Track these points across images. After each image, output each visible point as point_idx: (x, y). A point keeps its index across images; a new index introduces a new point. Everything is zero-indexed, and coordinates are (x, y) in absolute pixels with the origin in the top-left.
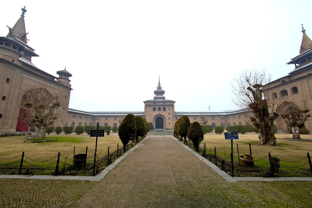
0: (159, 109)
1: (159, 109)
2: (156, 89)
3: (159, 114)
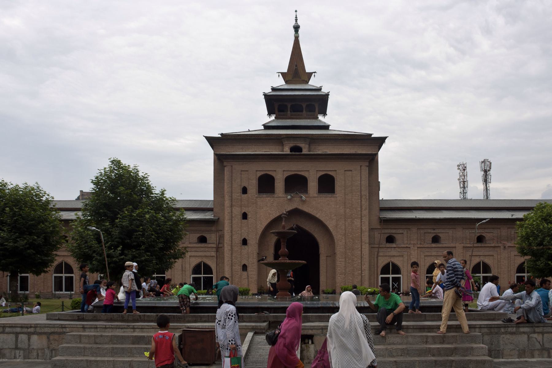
0: (296, 183)
1: (296, 183)
2: (280, 82)
3: (296, 213)
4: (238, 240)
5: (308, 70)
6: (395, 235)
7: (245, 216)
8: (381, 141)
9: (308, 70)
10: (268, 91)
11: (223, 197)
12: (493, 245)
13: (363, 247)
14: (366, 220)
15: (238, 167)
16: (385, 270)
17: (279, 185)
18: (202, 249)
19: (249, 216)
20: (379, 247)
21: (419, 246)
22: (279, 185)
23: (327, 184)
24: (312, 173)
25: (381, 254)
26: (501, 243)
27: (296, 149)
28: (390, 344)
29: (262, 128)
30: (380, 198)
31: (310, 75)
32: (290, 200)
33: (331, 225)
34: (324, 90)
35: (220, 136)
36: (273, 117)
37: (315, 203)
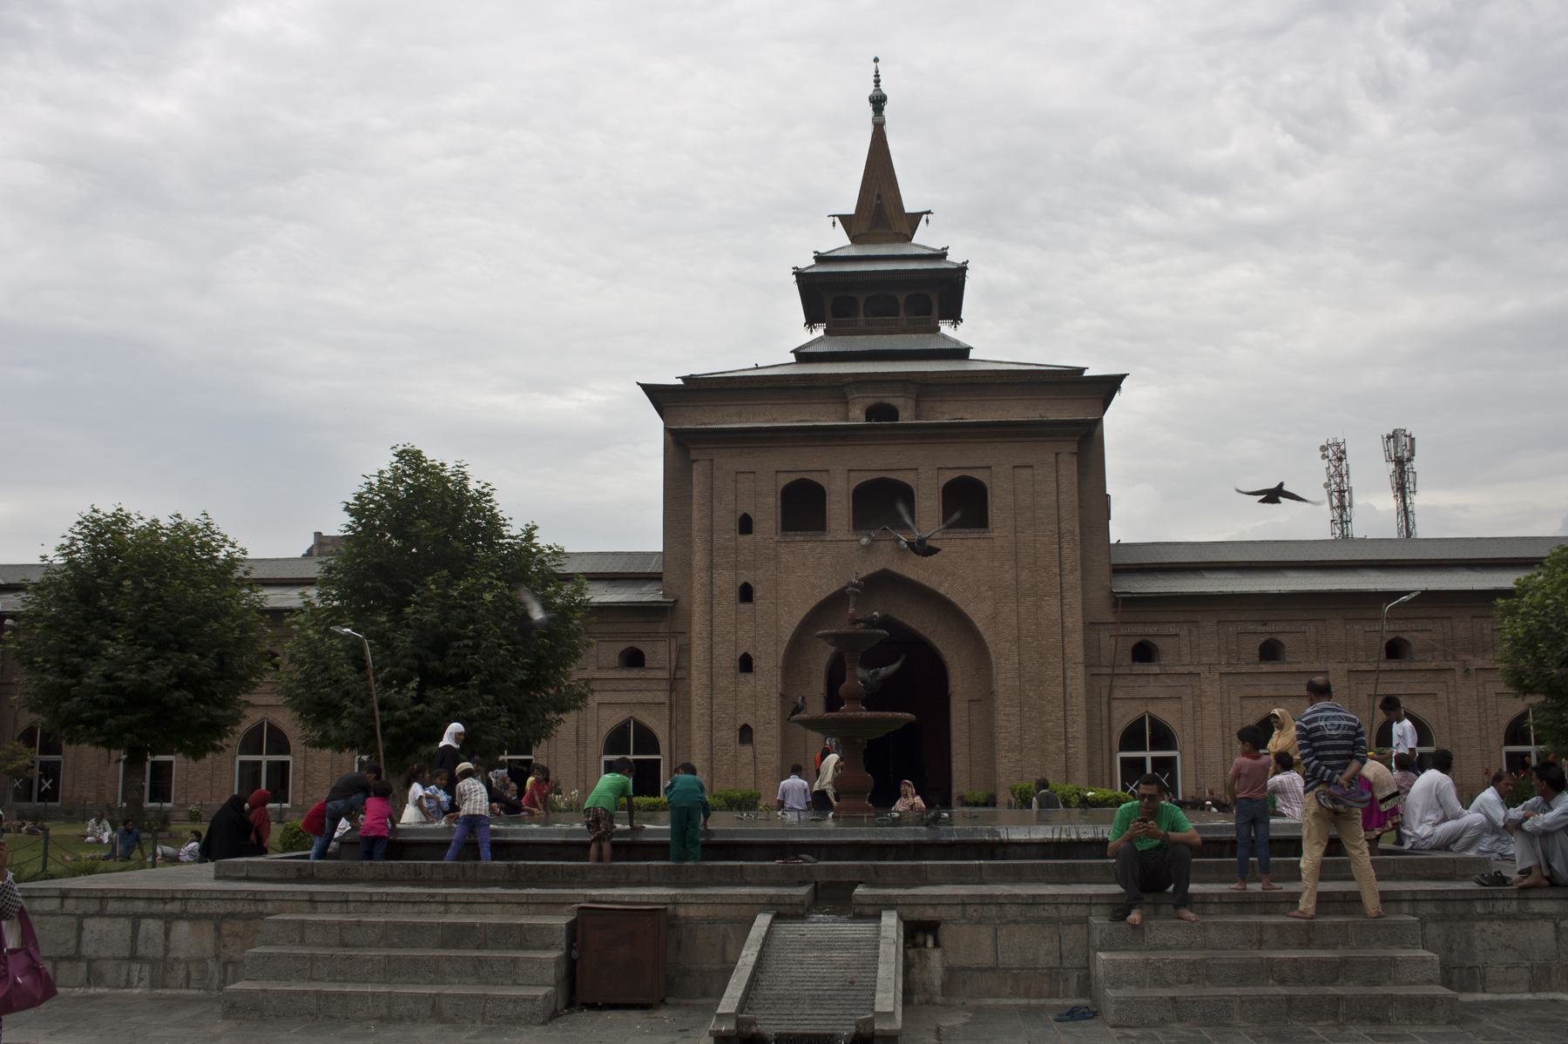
1: (880, 502)
2: (837, 240)
3: (884, 582)
4: (727, 658)
6: (1156, 641)
7: (746, 594)
8: (1110, 385)
10: (807, 262)
12: (1433, 665)
13: (1069, 673)
14: (1074, 600)
15: (729, 461)
16: (1132, 737)
17: (839, 508)
18: (632, 685)
19: (758, 593)
20: (1113, 675)
21: (1224, 669)
22: (839, 508)
23: (967, 503)
24: (927, 475)
25: (1118, 693)
26: (1454, 658)
28: (1154, 948)
29: (792, 359)
30: (1113, 540)
31: (915, 219)
32: (867, 547)
33: (978, 613)
34: (954, 258)
35: (680, 382)
36: (819, 332)
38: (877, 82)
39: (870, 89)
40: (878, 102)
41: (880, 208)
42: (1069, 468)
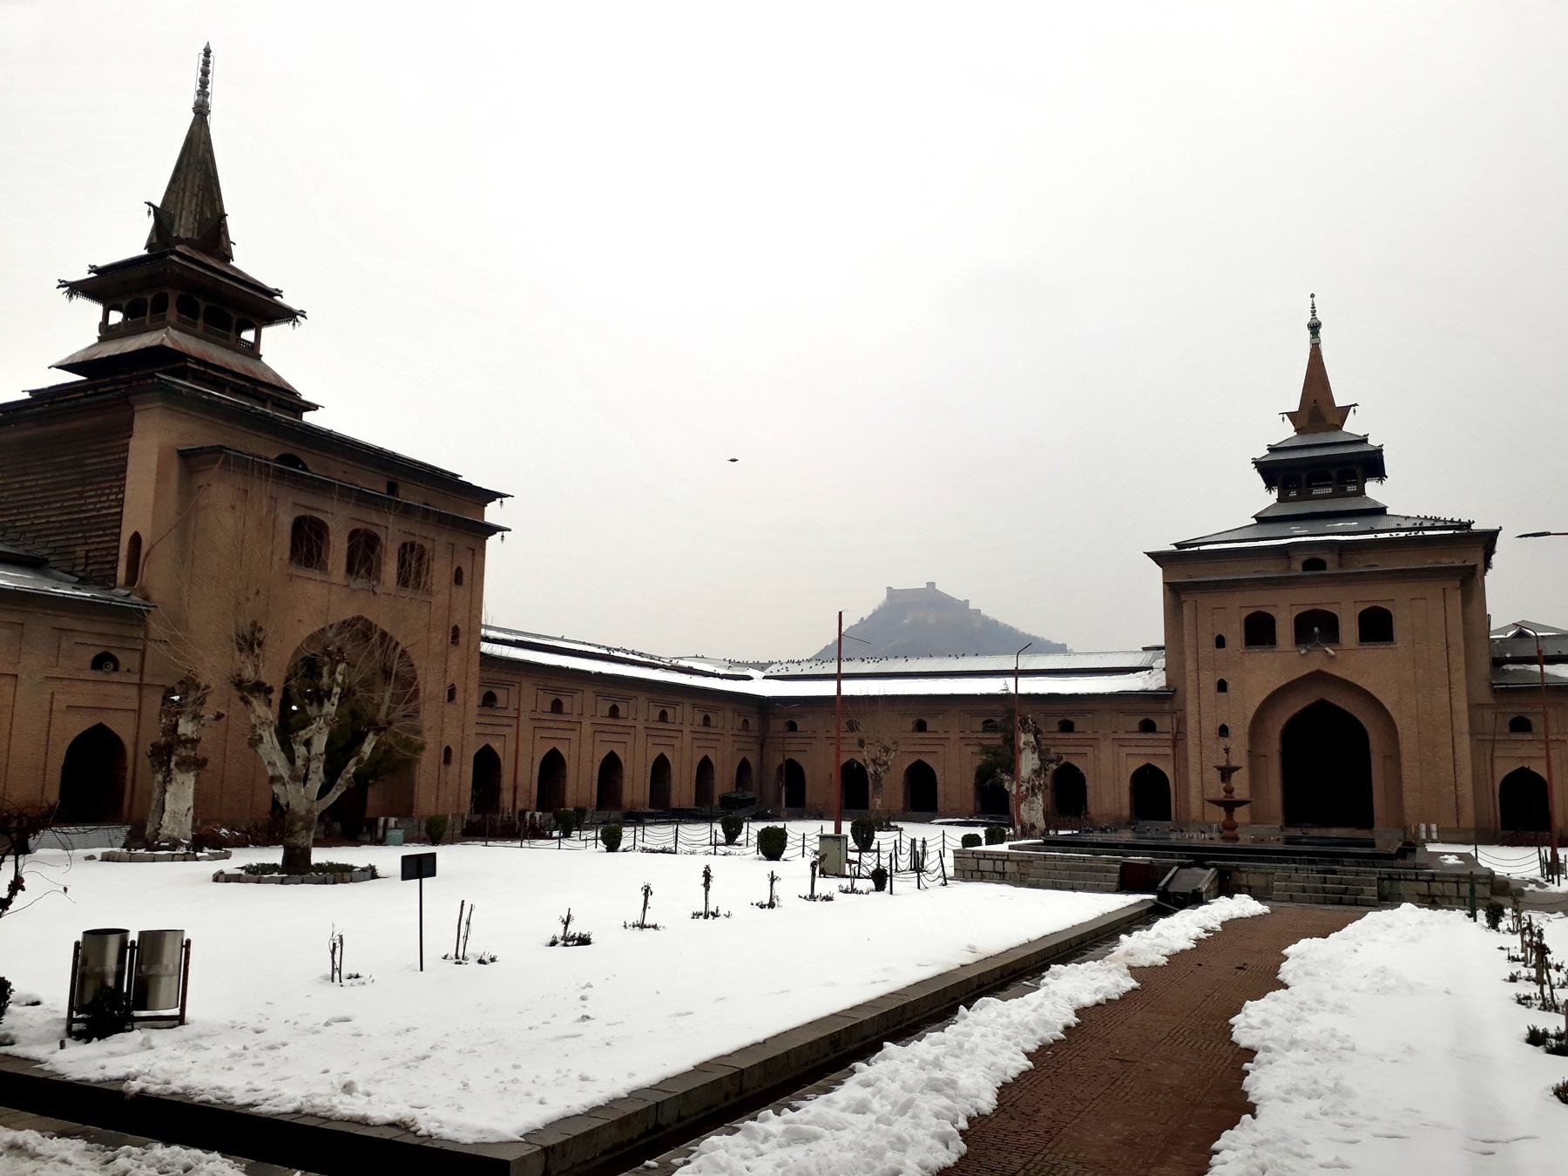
0: (1316, 627)
1: (1316, 627)
2: (1287, 431)
3: (1318, 677)
4: (1211, 728)
5: (1339, 402)
7: (1222, 686)
9: (1339, 402)
10: (1262, 452)
11: (1182, 653)
15: (1207, 601)
17: (1285, 630)
20: (1494, 741)
22: (1285, 630)
23: (1376, 627)
24: (1348, 609)
25: (1498, 753)
27: (1314, 564)
31: (1345, 410)
34: (1374, 442)
37: (1355, 662)
38: (1314, 313)
39: (1308, 318)
40: (1314, 328)
41: (1317, 407)
42: (1456, 599)
